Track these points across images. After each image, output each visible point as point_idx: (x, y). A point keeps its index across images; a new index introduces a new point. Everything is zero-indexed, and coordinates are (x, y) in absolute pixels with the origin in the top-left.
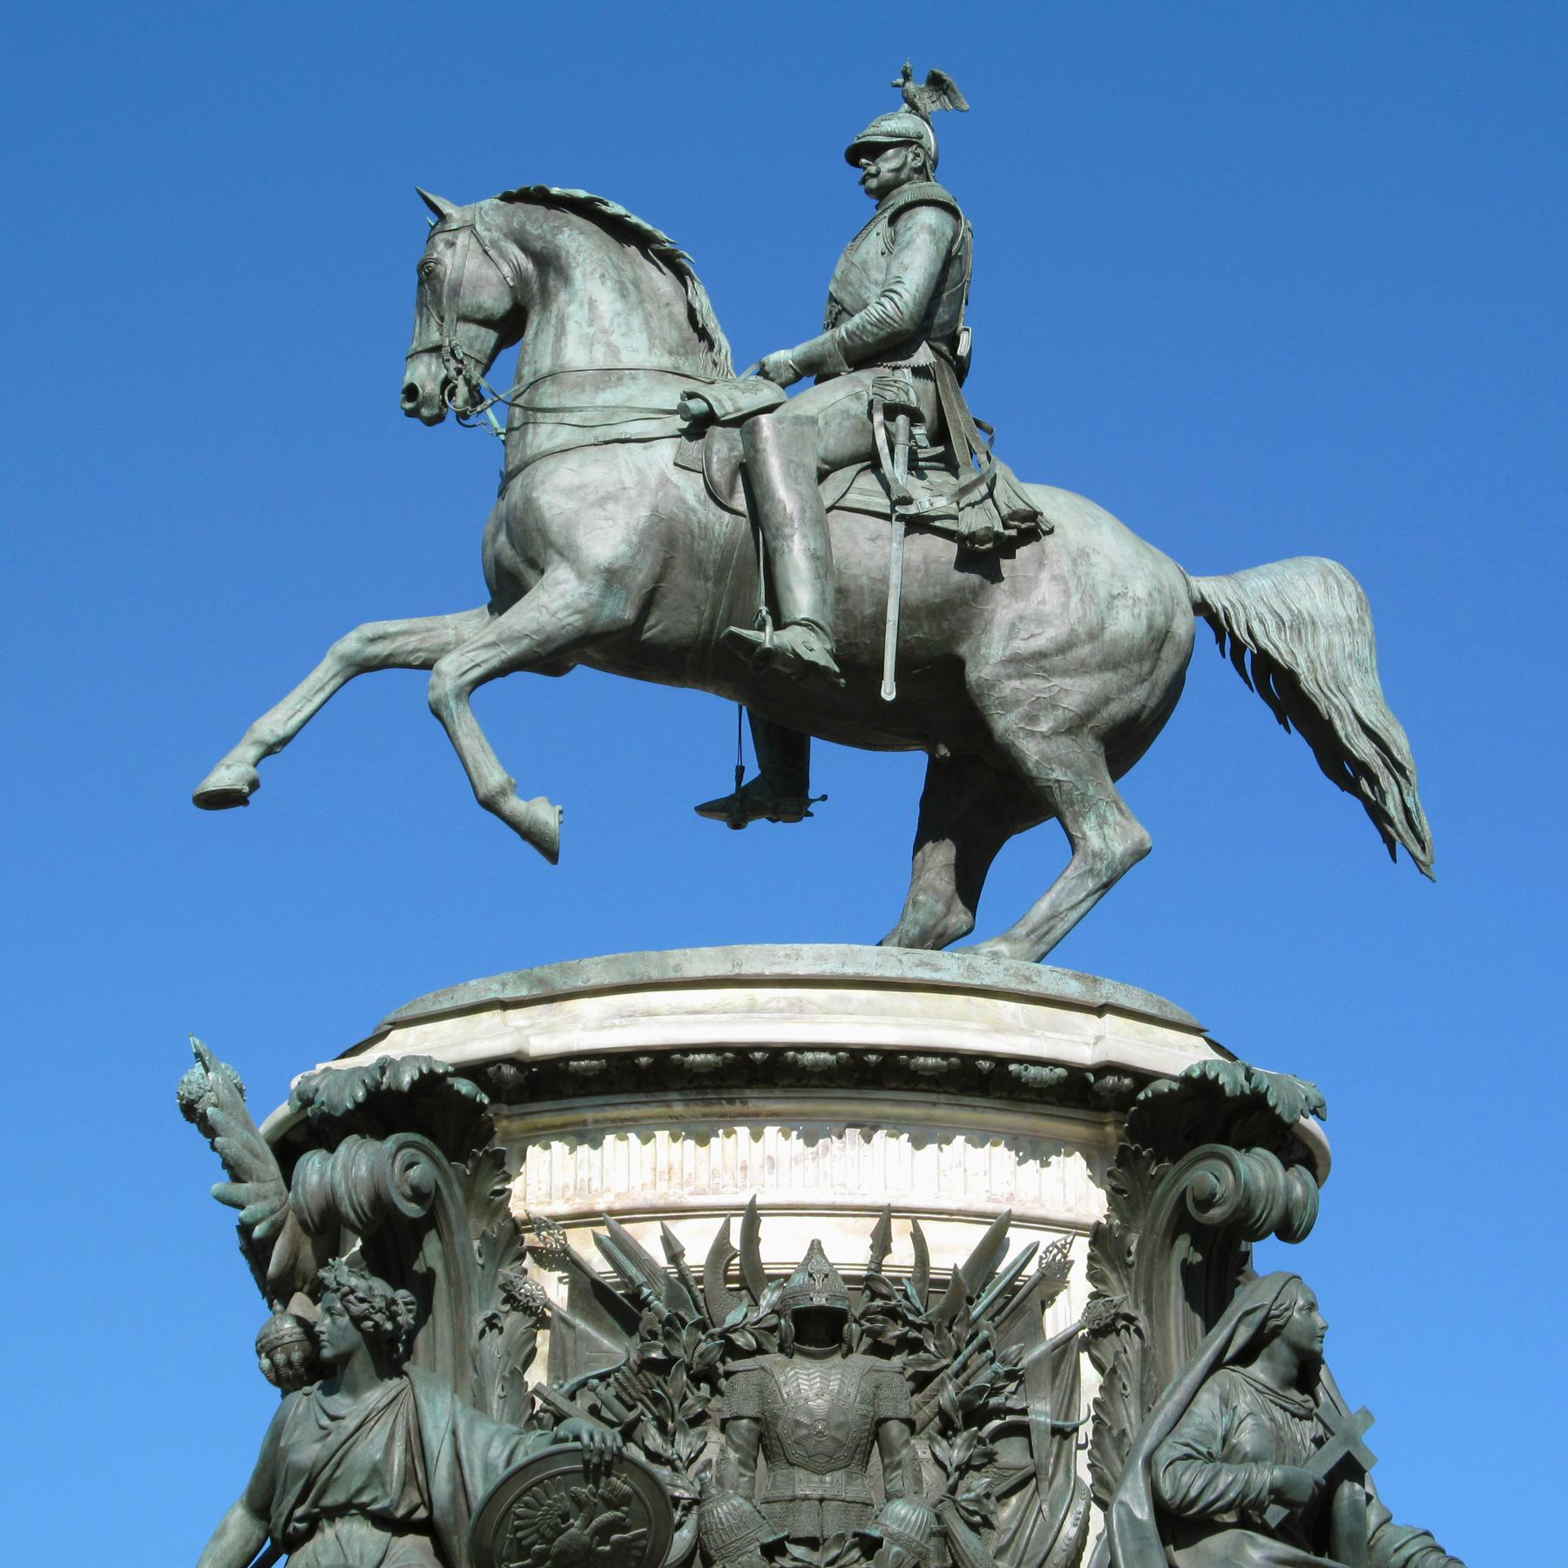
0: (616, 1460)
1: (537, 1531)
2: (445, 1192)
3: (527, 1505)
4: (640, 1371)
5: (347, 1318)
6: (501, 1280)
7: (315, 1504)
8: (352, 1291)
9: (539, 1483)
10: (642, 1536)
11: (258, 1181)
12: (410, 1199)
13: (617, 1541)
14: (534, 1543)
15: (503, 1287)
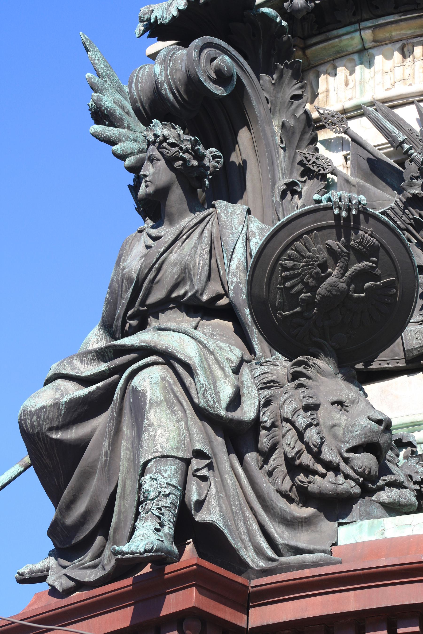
0: (362, 216)
1: (302, 281)
2: (245, 81)
3: (291, 258)
4: (406, 208)
5: (163, 161)
6: (299, 158)
7: (143, 303)
8: (165, 139)
9: (299, 238)
10: (390, 285)
11: (129, 128)
12: (214, 82)
13: (370, 287)
14: (301, 292)
15: (301, 163)
